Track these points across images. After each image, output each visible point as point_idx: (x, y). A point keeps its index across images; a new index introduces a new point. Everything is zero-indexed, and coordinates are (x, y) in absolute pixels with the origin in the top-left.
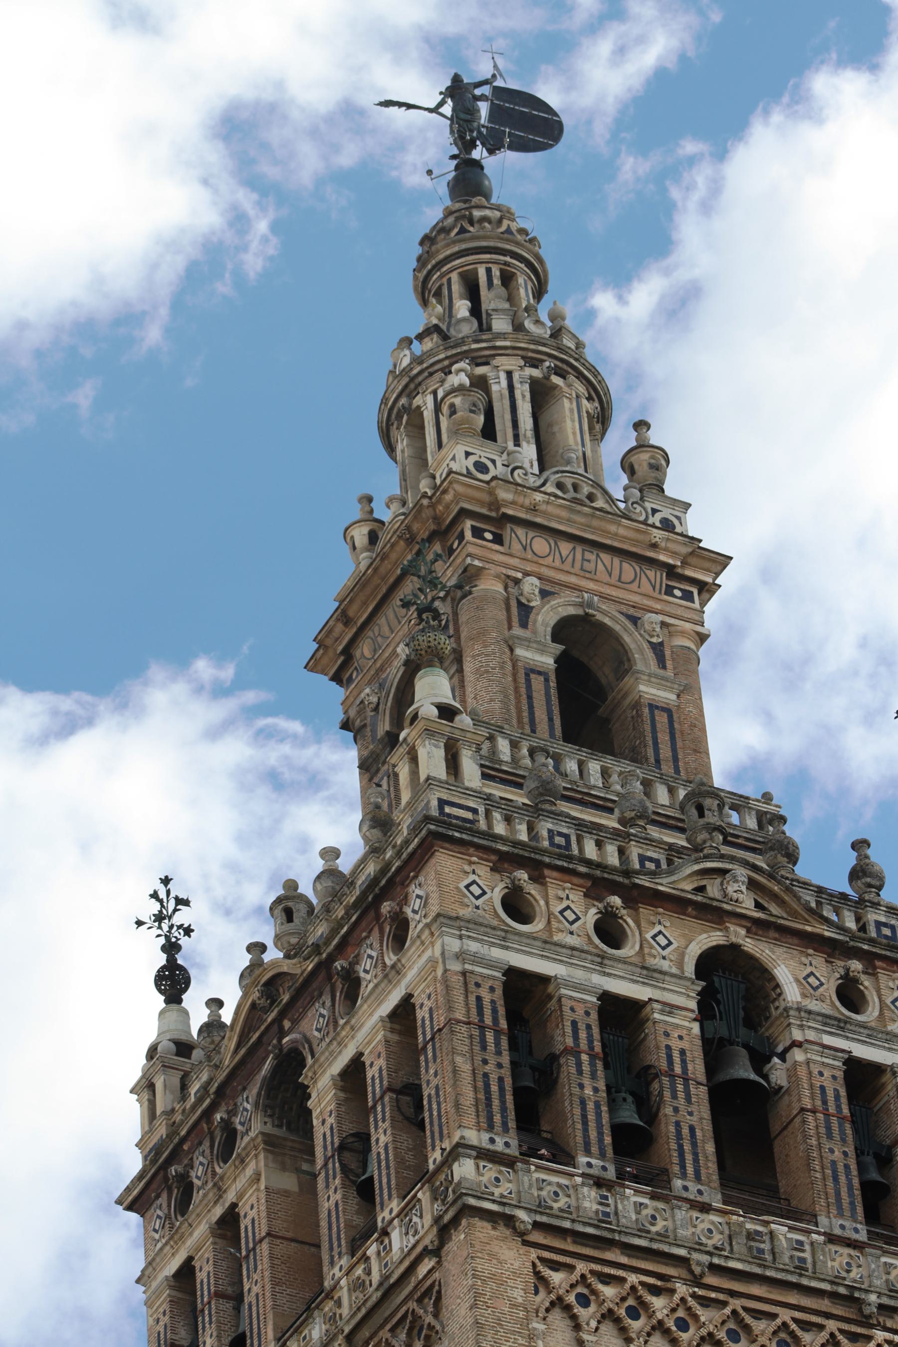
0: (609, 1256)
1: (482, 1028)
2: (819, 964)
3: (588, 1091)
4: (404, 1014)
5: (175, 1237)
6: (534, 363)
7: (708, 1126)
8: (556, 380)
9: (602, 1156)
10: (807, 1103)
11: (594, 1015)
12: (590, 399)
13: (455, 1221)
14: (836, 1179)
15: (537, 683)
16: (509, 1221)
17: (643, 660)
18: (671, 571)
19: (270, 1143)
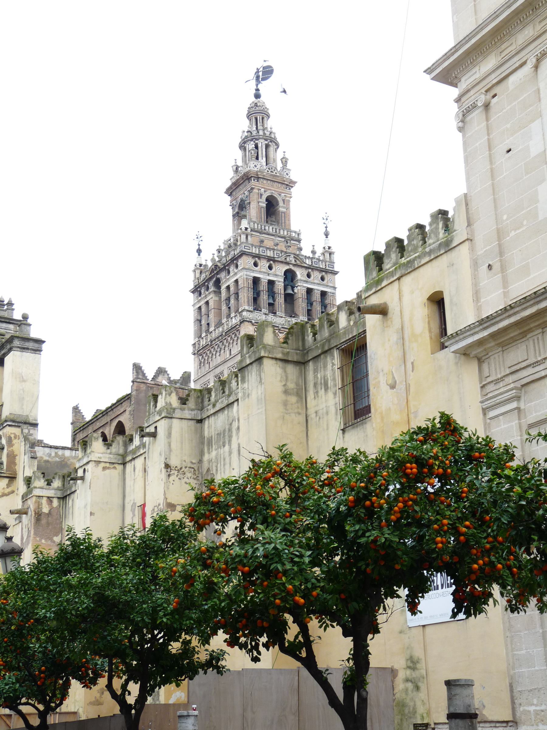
4: (236, 281)
5: (199, 301)
6: (266, 140)
7: (283, 302)
8: (270, 143)
10: (300, 296)
13: (243, 321)
15: (263, 210)
16: (251, 322)
17: (281, 204)
18: (287, 185)
19: (215, 292)
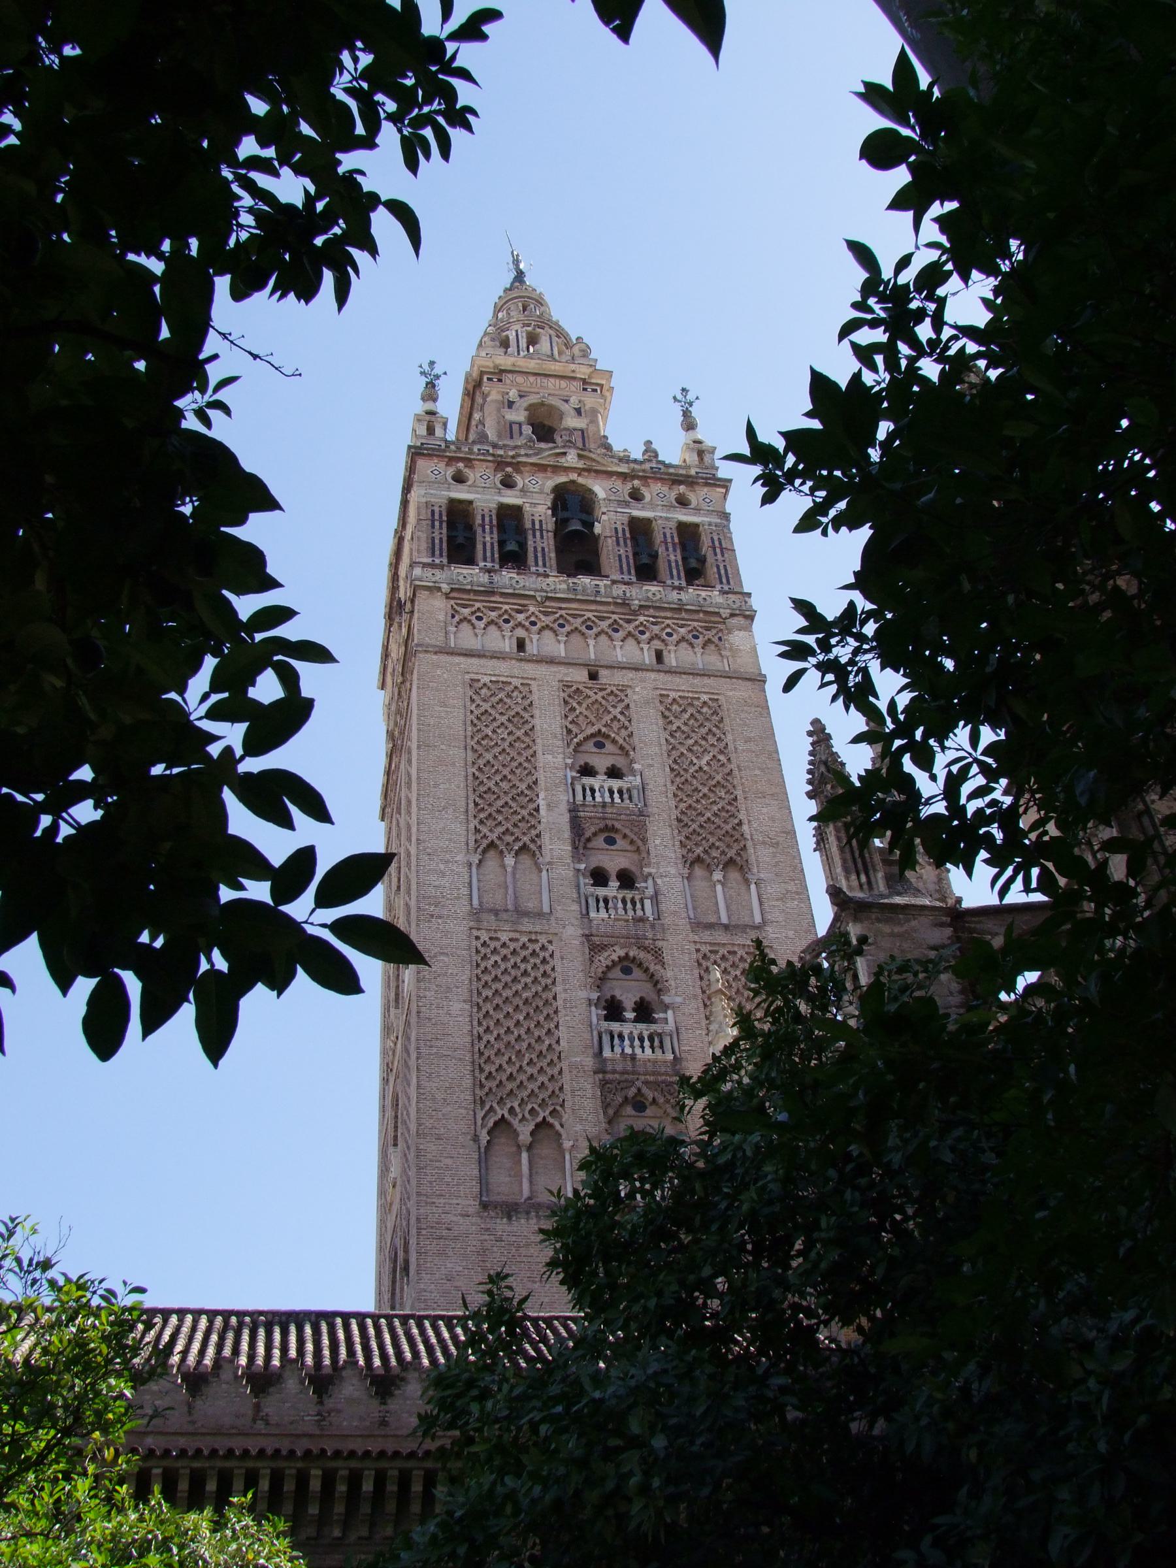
0: (493, 599)
1: (433, 521)
2: (618, 484)
3: (488, 539)
7: (552, 547)
9: (493, 561)
11: (494, 512)
12: (558, 337)
14: (620, 560)
16: (439, 589)
18: (584, 381)
